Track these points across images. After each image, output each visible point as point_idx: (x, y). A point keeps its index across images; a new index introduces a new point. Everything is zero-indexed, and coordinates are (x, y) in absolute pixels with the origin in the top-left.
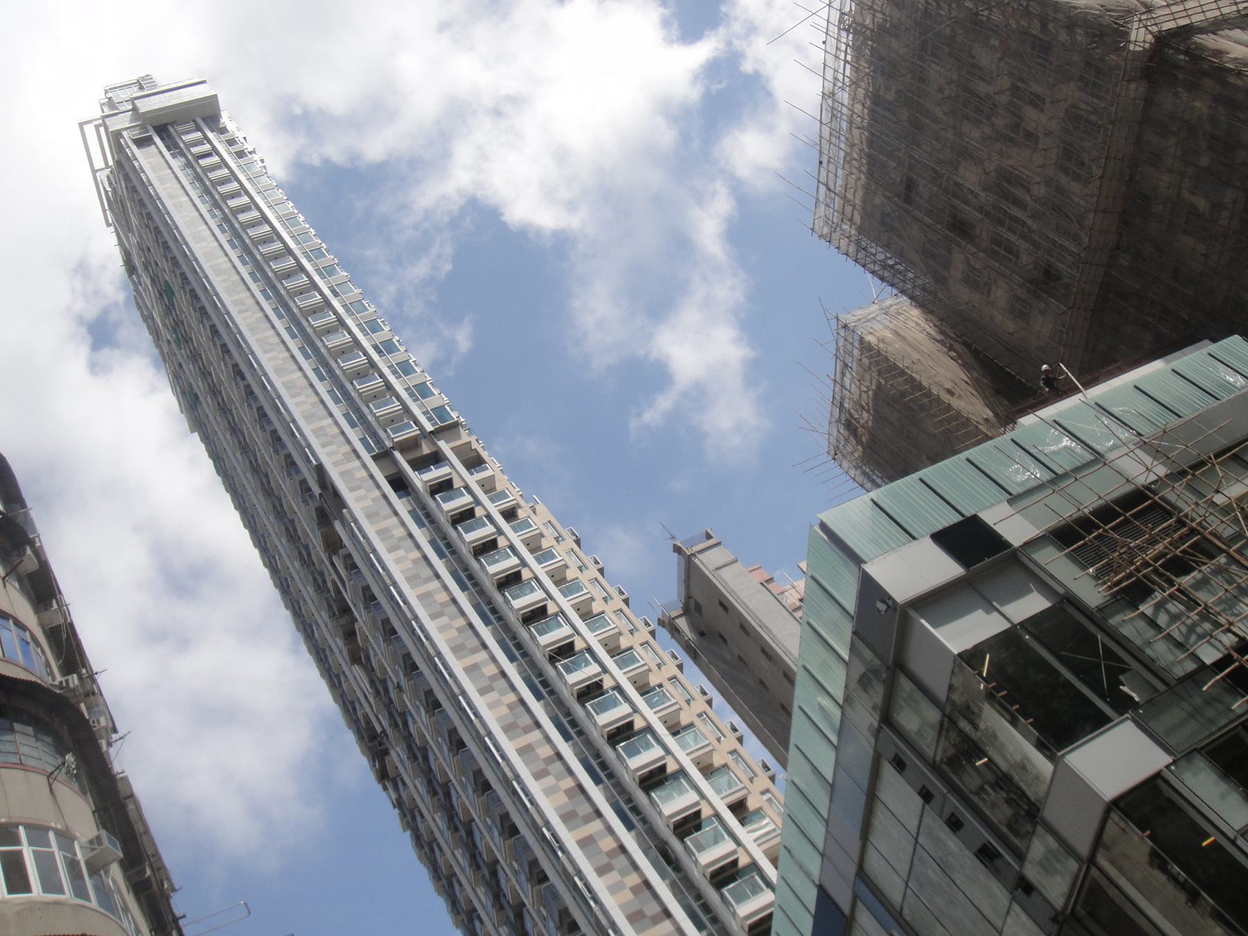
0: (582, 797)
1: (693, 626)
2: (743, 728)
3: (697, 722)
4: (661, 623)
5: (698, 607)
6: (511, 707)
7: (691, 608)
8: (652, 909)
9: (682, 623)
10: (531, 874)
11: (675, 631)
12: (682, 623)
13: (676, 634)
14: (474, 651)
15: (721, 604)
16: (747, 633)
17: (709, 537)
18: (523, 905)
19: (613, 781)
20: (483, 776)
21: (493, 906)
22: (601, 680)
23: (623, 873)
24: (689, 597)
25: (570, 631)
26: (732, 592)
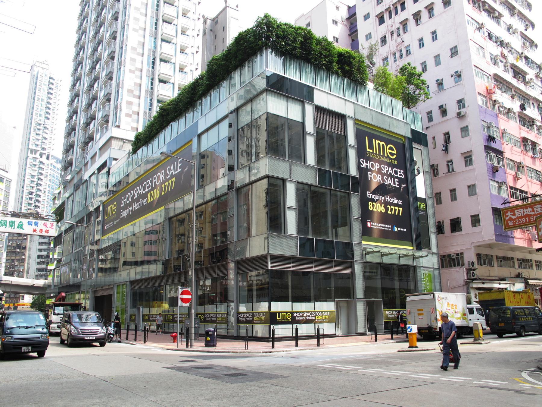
0: (142, 47)
1: (211, 25)
2: (200, 50)
3: (191, 36)
4: (203, 16)
5: (217, 22)
6: (136, 84)
7: (215, 21)
8: (137, 93)
9: (209, 22)
10: (110, 54)
11: (205, 22)
12: (209, 22)
13: (204, 23)
14: (135, 96)
15: (224, 28)
16: (224, 30)
17: (237, 6)
18: (100, 60)
19: (150, 112)
20: (110, 96)
21: (91, 52)
22: (174, 20)
23: (133, 121)
24: (217, 17)
25: (172, 74)
26: (229, 27)
